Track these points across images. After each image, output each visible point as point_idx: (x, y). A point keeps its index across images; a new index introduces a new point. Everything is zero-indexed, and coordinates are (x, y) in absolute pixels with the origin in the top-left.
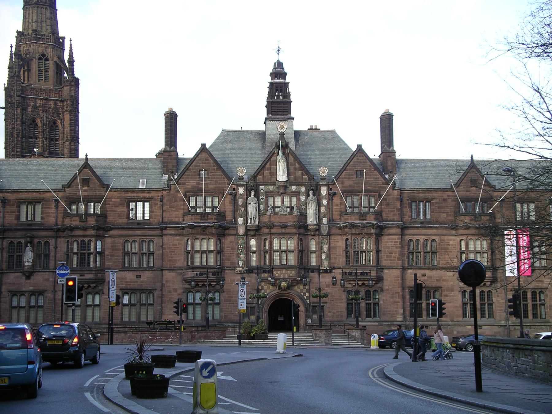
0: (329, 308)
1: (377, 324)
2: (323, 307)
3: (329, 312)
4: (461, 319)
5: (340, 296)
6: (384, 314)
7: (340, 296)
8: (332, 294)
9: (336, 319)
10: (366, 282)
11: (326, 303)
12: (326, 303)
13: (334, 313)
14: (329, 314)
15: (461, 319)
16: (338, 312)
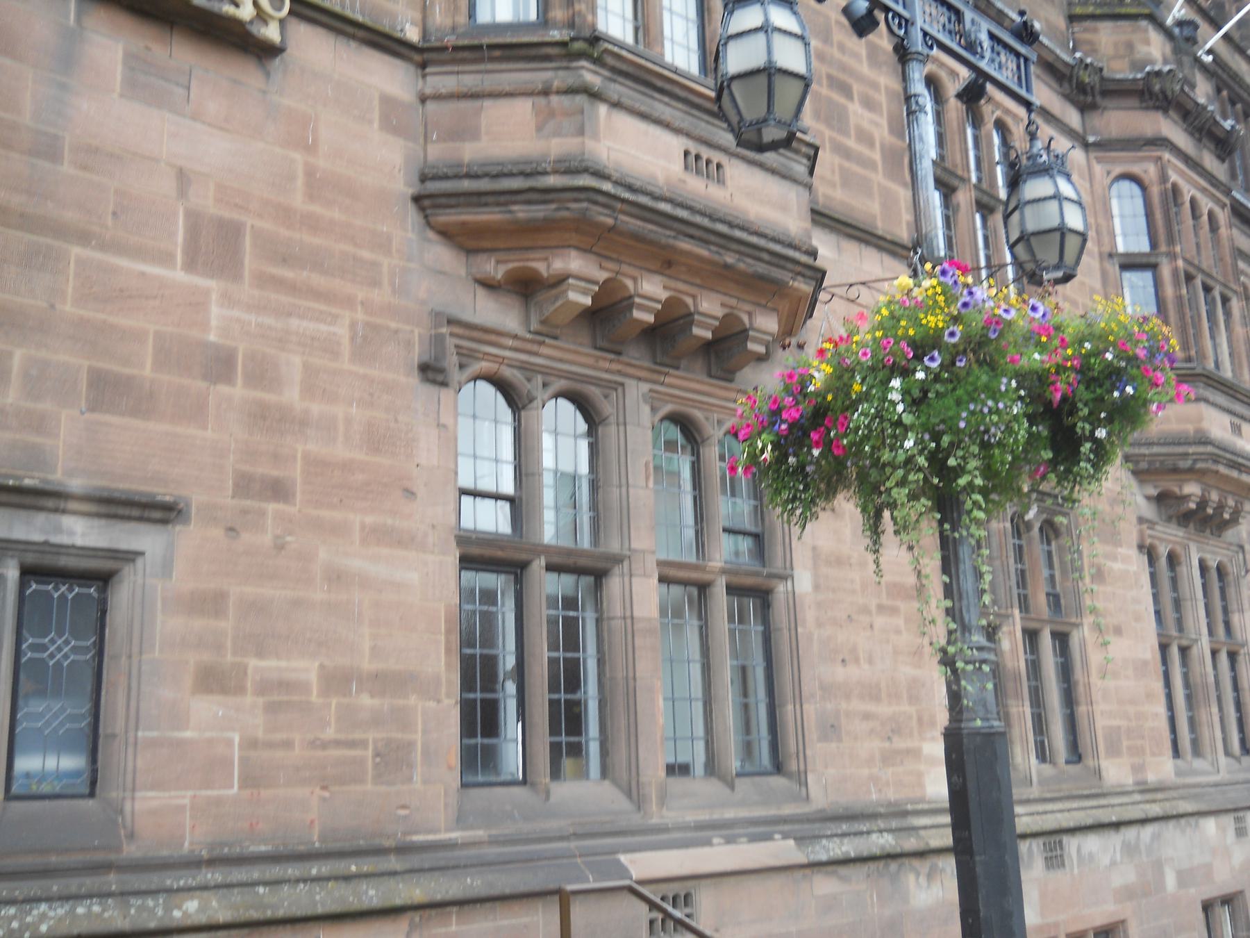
0: (210, 604)
1: (783, 850)
2: (100, 576)
3: (213, 680)
4: (1163, 768)
5: (376, 440)
6: (831, 730)
7: (376, 440)
8: (263, 374)
9: (307, 811)
10: (710, 306)
11: (162, 512)
12: (162, 512)
13: (280, 695)
14: (207, 719)
15: (1163, 768)
16: (337, 681)
